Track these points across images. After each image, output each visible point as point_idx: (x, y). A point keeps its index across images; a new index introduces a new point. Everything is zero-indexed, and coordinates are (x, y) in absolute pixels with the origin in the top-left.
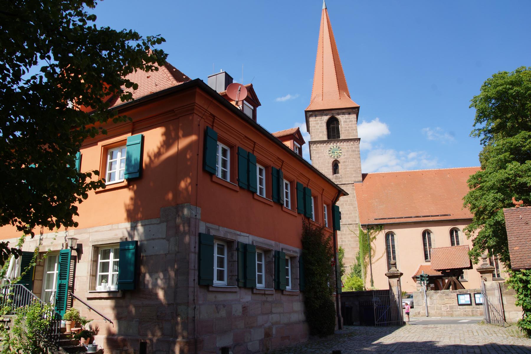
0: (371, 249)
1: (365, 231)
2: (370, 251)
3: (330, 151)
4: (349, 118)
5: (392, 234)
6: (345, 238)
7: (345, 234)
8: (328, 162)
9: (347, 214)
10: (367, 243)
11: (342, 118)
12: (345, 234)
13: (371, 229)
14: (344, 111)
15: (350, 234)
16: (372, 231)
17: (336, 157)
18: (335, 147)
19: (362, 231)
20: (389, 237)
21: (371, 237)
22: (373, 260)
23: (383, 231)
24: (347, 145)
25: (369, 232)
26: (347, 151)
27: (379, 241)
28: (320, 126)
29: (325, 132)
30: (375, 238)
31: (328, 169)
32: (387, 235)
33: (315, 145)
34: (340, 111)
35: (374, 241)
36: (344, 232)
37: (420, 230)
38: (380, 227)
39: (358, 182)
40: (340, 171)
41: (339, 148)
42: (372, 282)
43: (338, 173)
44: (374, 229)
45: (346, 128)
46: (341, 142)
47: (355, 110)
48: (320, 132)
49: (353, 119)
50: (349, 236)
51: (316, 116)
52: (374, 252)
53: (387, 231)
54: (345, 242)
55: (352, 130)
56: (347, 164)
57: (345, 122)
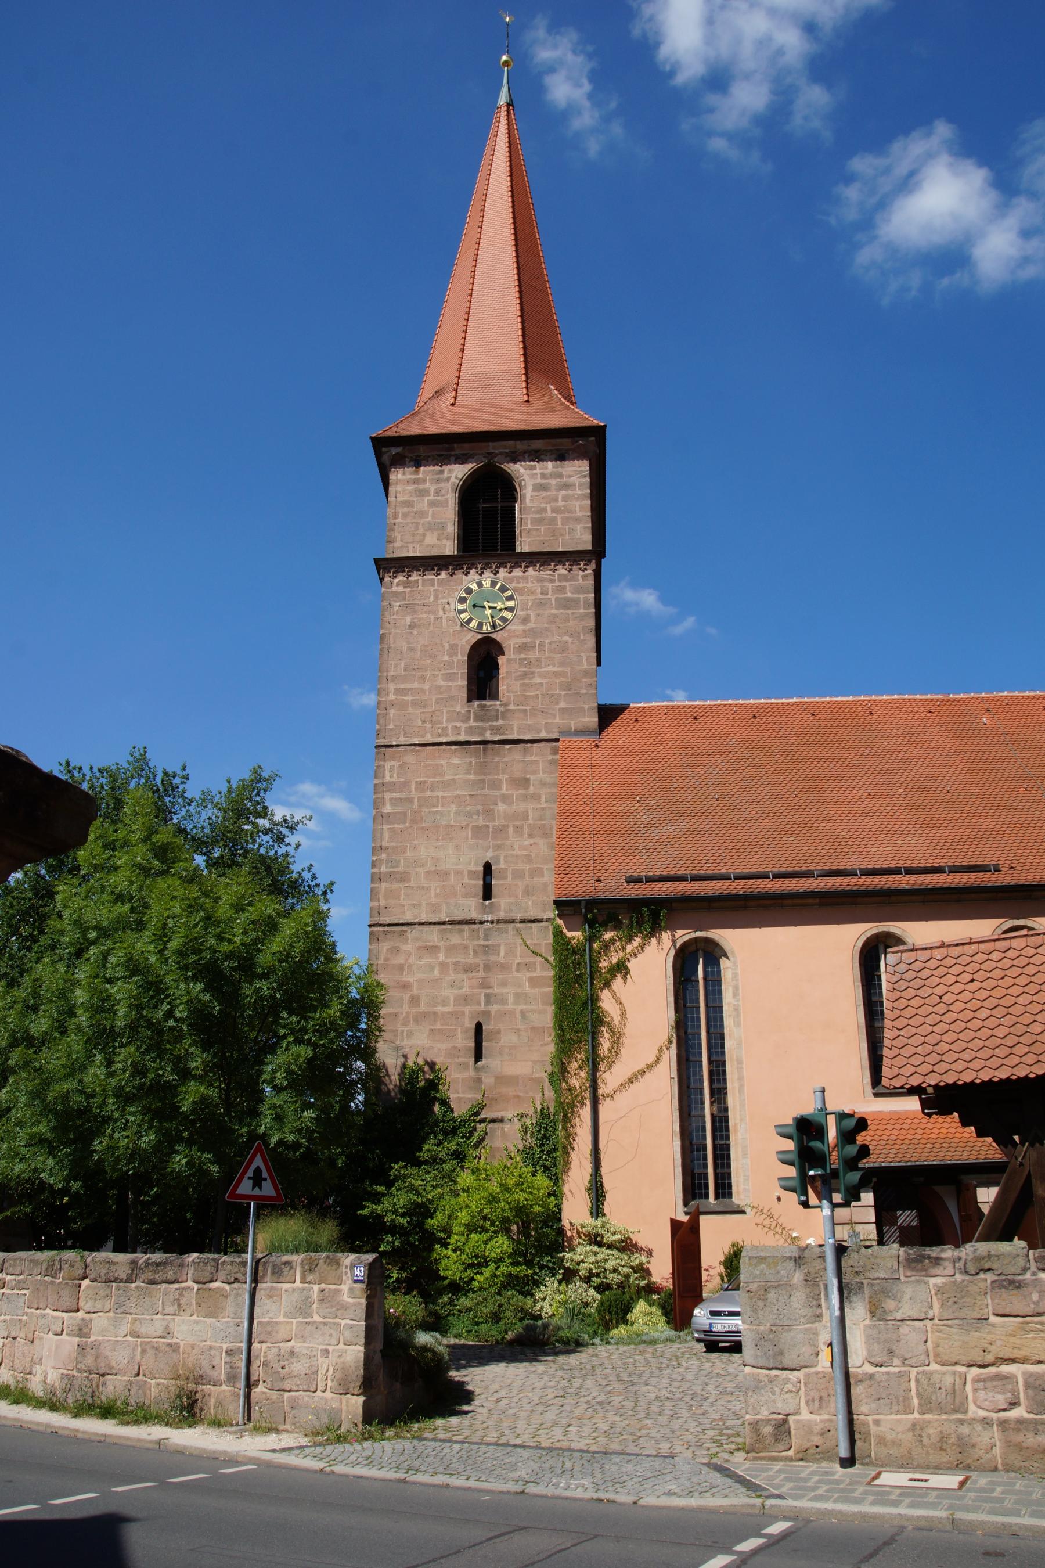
1: (576, 935)
2: (595, 1035)
3: (462, 600)
4: (560, 476)
5: (713, 953)
6: (504, 984)
7: (504, 967)
8: (453, 648)
9: (518, 875)
10: (582, 994)
11: (527, 475)
12: (504, 967)
14: (538, 444)
15: (528, 966)
16: (608, 935)
17: (487, 628)
18: (487, 584)
19: (558, 934)
21: (604, 964)
22: (610, 1079)
23: (666, 936)
24: (540, 580)
25: (591, 939)
26: (540, 604)
27: (642, 987)
28: (432, 504)
29: (452, 528)
30: (621, 968)
31: (450, 677)
32: (684, 962)
33: (400, 578)
34: (520, 445)
35: (618, 983)
36: (501, 958)
37: (847, 937)
38: (645, 914)
39: (577, 733)
40: (502, 688)
41: (503, 589)
42: (597, 1192)
43: (495, 696)
44: (617, 927)
45: (544, 510)
46: (517, 565)
47: (587, 443)
48: (430, 527)
49: (575, 480)
50: (524, 976)
51: (418, 464)
52: (617, 1040)
53: (683, 935)
54: (503, 1001)
55: (566, 521)
56: (532, 655)
57: (539, 488)
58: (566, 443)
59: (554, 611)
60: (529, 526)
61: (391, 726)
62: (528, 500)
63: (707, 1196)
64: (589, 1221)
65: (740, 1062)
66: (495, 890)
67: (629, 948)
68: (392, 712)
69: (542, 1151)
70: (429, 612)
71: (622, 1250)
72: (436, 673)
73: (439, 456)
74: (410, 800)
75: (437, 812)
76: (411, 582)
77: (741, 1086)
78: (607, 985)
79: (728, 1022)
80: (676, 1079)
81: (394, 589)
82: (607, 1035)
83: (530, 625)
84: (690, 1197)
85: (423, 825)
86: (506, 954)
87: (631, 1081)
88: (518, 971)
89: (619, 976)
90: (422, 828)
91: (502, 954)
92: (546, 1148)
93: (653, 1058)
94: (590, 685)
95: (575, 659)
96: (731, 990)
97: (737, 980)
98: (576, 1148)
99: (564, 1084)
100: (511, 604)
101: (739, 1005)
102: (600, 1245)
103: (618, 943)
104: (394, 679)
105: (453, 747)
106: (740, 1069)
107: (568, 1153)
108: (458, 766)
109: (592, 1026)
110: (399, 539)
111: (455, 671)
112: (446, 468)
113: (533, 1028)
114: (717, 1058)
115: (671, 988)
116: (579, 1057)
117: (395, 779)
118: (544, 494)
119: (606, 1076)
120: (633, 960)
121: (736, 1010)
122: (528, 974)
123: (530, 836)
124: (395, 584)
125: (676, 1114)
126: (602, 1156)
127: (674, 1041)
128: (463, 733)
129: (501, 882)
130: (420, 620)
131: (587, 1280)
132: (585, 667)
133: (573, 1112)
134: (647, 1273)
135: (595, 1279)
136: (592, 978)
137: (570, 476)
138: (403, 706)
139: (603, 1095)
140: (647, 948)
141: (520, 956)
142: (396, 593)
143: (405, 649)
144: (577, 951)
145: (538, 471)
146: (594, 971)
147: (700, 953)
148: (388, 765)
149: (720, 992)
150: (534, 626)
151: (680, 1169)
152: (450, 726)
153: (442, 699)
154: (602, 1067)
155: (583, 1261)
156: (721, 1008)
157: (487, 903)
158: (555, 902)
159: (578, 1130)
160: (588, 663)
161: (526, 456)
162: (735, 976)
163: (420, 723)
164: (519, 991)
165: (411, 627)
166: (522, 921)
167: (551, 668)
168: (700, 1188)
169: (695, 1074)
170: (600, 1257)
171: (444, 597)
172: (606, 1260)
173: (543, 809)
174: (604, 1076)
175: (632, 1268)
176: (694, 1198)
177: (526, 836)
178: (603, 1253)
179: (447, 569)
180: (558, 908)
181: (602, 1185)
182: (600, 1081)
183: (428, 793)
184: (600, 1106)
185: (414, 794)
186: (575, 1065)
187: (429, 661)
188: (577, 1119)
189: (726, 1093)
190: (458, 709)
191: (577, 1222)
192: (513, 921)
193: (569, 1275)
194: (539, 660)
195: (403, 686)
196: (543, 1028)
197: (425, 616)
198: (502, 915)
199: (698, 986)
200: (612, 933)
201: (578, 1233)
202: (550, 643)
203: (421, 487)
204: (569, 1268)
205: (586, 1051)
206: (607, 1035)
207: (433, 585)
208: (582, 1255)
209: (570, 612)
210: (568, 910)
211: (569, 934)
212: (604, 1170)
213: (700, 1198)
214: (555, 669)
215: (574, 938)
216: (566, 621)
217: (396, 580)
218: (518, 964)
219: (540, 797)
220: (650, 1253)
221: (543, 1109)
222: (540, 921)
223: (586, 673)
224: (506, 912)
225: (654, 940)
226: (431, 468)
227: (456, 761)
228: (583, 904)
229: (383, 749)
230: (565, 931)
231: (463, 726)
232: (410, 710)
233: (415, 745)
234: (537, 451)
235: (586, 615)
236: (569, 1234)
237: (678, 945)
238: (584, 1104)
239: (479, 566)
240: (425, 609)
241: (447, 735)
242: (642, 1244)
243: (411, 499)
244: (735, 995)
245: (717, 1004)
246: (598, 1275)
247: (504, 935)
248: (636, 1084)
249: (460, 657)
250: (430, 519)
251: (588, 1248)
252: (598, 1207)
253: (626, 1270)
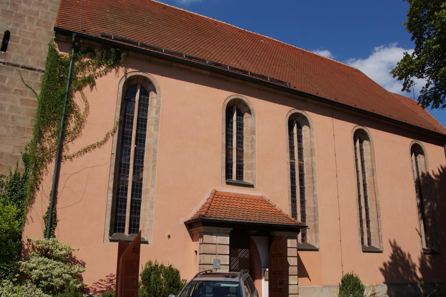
0: (70, 109)
1: (65, 55)
2: (66, 117)
5: (147, 88)
9: (26, 42)
10: (62, 91)
13: (85, 53)
16: (86, 60)
19: (52, 50)
20: (136, 93)
21: (80, 76)
22: (72, 147)
25: (75, 59)
30: (91, 81)
35: (87, 89)
37: (220, 97)
38: (113, 51)
44: (93, 56)
50: (18, 98)
52: (80, 123)
53: (132, 72)
63: (123, 231)
64: (42, 239)
65: (155, 151)
66: (9, 47)
67: (98, 71)
69: (11, 199)
71: (65, 262)
77: (154, 166)
78: (80, 89)
79: (150, 128)
80: (115, 155)
82: (74, 119)
84: (113, 230)
86: (9, 83)
87: (86, 150)
88: (15, 93)
89: (88, 87)
91: (7, 82)
92: (14, 197)
93: (102, 139)
96: (154, 110)
97: (160, 105)
98: (41, 188)
99: (38, 145)
101: (159, 119)
102: (49, 257)
103: (91, 66)
106: (154, 156)
107: (34, 191)
109: (66, 111)
113: (18, 127)
114: (140, 148)
115: (120, 100)
116: (53, 129)
119: (70, 144)
120: (99, 78)
121: (157, 121)
122: (21, 97)
123: (37, 24)
125: (112, 176)
126: (58, 197)
127: (117, 131)
129: (15, 44)
131: (37, 282)
133: (42, 165)
134: (80, 278)
135: (43, 282)
136: (71, 82)
139: (65, 156)
140: (109, 74)
141: (18, 85)
144: (64, 64)
146: (72, 79)
147: (139, 86)
149: (147, 111)
151: (110, 211)
154: (68, 138)
155: (36, 269)
156: (146, 120)
157: (3, 52)
158: (56, 29)
159: (44, 177)
162: (158, 102)
164: (13, 104)
166: (23, 67)
168: (120, 225)
169: (125, 156)
170: (49, 266)
172: (54, 268)
173: (48, 13)
174: (68, 144)
175: (71, 274)
176: (115, 232)
177: (35, 24)
178: (52, 263)
180: (56, 35)
181: (55, 216)
182: (64, 147)
184: (62, 163)
186: (50, 134)
188: (45, 170)
189: (142, 170)
191: (34, 239)
192: (17, 66)
193: (23, 278)
196: (25, 128)
198: (11, 61)
199: (134, 105)
200: (88, 59)
201: (33, 246)
204: (22, 272)
205: (58, 126)
206: (74, 119)
208: (34, 264)
210: (63, 37)
211: (60, 53)
212: (58, 206)
213: (119, 231)
215: (63, 56)
218: (16, 90)
219: (47, 7)
220: (83, 265)
221: (16, 174)
222: (35, 70)
224: (14, 60)
225: (114, 70)
228: (74, 35)
230: (57, 49)
236: (26, 247)
237: (128, 76)
238: (50, 160)
242: (79, 258)
244: (157, 112)
245: (144, 117)
246: (46, 279)
247: (10, 72)
248: (88, 153)
251: (40, 259)
252: (51, 230)
253: (68, 276)
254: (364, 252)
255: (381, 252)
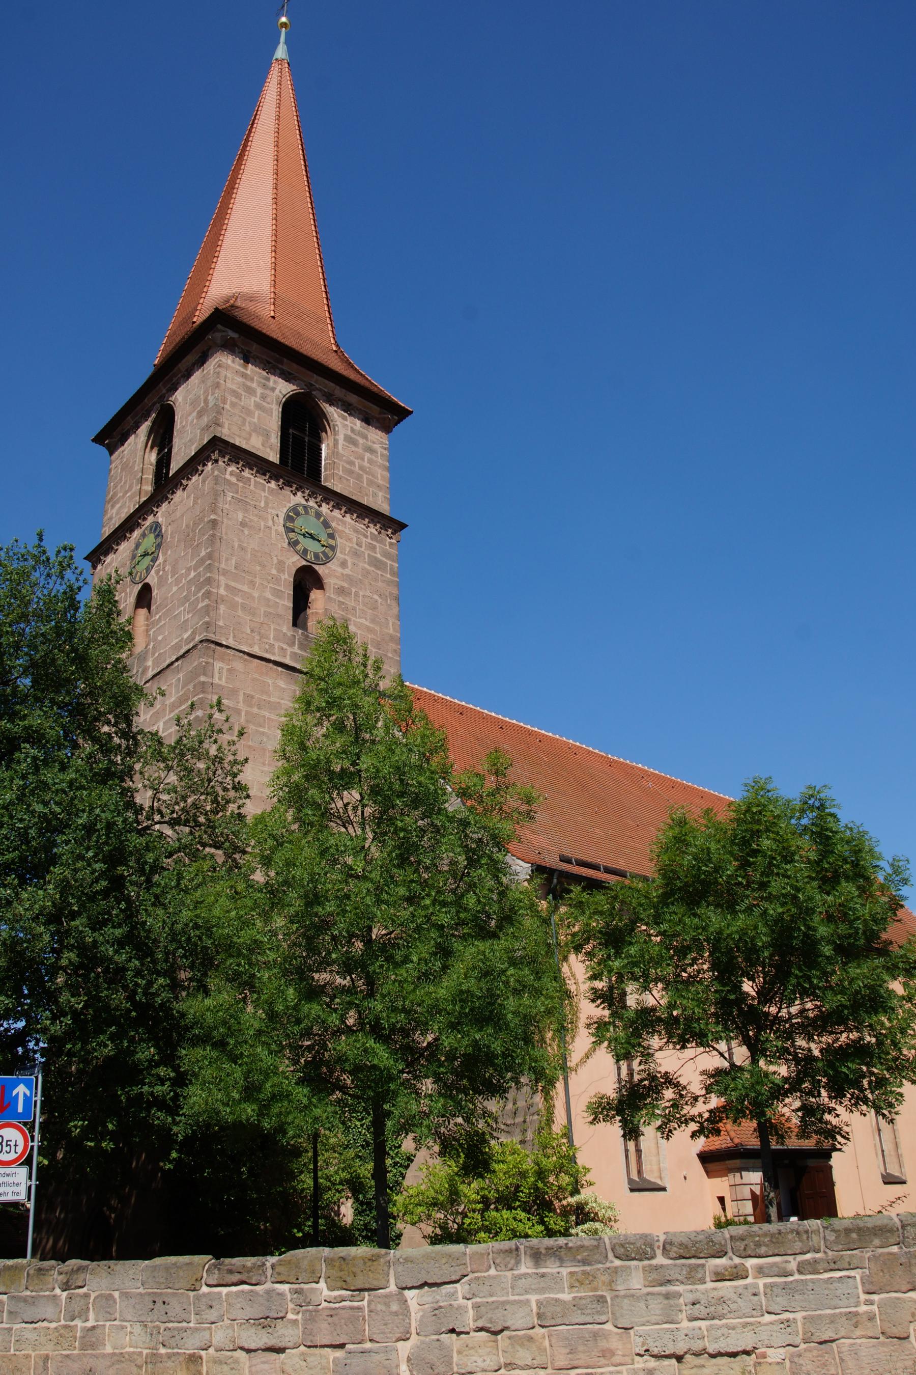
8: (281, 563)
14: (353, 399)
24: (356, 531)
28: (258, 406)
33: (233, 468)
34: (339, 392)
45: (352, 463)
58: (374, 409)
59: (366, 566)
60: (341, 473)
61: (221, 623)
62: (340, 447)
68: (222, 608)
70: (260, 517)
72: (265, 583)
73: (269, 363)
74: (238, 712)
75: (263, 734)
76: (244, 477)
81: (228, 476)
83: (347, 571)
85: (250, 743)
90: (249, 747)
94: (395, 651)
95: (383, 620)
100: (331, 542)
104: (225, 573)
105: (280, 669)
108: (283, 690)
110: (226, 426)
111: (282, 589)
112: (273, 378)
117: (223, 682)
118: (353, 449)
124: (228, 472)
128: (288, 657)
130: (251, 521)
132: (391, 631)
137: (374, 443)
138: (233, 606)
142: (229, 482)
143: (236, 545)
145: (348, 423)
148: (218, 665)
150: (350, 573)
152: (277, 645)
153: (270, 613)
160: (394, 629)
161: (340, 403)
163: (249, 631)
165: (243, 524)
167: (363, 621)
171: (273, 508)
179: (277, 480)
183: (255, 710)
185: (241, 705)
187: (258, 568)
190: (285, 629)
194: (354, 609)
195: (233, 584)
197: (256, 519)
202: (364, 596)
203: (249, 383)
207: (264, 491)
209: (379, 572)
214: (367, 623)
216: (376, 580)
217: (230, 469)
223: (392, 638)
226: (257, 369)
227: (282, 684)
229: (213, 646)
231: (289, 650)
232: (240, 613)
233: (244, 652)
234: (350, 405)
235: (392, 581)
239: (307, 492)
240: (256, 512)
241: (274, 654)
243: (239, 391)
249: (286, 576)
250: (255, 420)
254: (885, 1183)
255: (904, 1183)
